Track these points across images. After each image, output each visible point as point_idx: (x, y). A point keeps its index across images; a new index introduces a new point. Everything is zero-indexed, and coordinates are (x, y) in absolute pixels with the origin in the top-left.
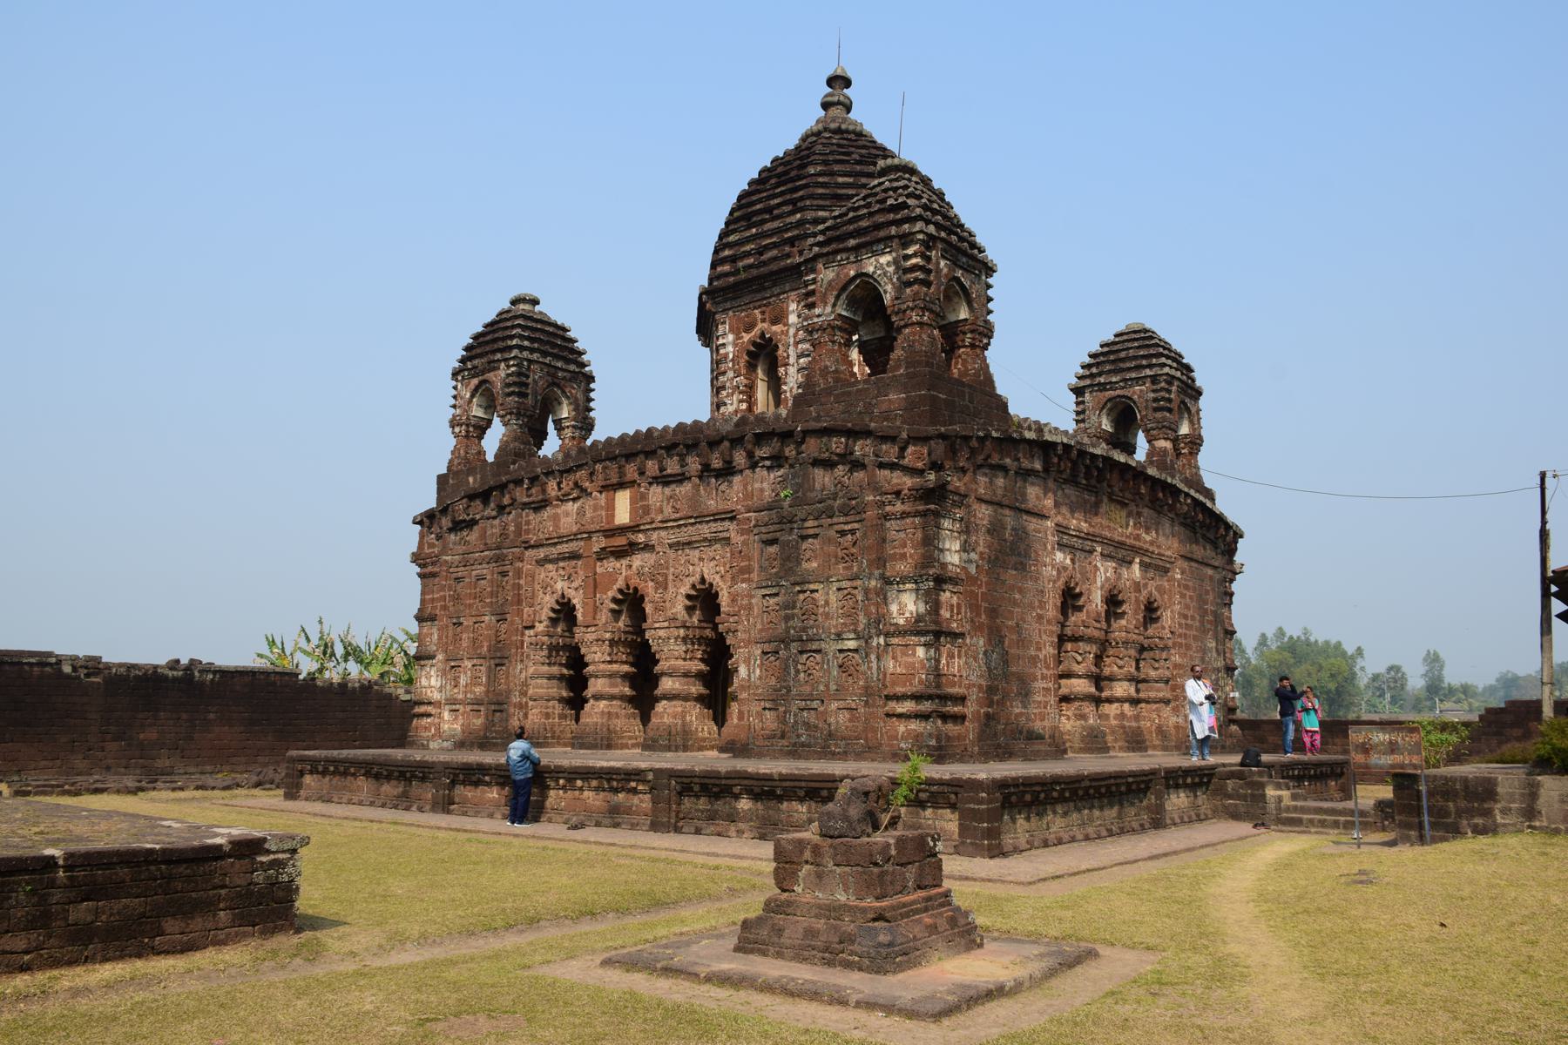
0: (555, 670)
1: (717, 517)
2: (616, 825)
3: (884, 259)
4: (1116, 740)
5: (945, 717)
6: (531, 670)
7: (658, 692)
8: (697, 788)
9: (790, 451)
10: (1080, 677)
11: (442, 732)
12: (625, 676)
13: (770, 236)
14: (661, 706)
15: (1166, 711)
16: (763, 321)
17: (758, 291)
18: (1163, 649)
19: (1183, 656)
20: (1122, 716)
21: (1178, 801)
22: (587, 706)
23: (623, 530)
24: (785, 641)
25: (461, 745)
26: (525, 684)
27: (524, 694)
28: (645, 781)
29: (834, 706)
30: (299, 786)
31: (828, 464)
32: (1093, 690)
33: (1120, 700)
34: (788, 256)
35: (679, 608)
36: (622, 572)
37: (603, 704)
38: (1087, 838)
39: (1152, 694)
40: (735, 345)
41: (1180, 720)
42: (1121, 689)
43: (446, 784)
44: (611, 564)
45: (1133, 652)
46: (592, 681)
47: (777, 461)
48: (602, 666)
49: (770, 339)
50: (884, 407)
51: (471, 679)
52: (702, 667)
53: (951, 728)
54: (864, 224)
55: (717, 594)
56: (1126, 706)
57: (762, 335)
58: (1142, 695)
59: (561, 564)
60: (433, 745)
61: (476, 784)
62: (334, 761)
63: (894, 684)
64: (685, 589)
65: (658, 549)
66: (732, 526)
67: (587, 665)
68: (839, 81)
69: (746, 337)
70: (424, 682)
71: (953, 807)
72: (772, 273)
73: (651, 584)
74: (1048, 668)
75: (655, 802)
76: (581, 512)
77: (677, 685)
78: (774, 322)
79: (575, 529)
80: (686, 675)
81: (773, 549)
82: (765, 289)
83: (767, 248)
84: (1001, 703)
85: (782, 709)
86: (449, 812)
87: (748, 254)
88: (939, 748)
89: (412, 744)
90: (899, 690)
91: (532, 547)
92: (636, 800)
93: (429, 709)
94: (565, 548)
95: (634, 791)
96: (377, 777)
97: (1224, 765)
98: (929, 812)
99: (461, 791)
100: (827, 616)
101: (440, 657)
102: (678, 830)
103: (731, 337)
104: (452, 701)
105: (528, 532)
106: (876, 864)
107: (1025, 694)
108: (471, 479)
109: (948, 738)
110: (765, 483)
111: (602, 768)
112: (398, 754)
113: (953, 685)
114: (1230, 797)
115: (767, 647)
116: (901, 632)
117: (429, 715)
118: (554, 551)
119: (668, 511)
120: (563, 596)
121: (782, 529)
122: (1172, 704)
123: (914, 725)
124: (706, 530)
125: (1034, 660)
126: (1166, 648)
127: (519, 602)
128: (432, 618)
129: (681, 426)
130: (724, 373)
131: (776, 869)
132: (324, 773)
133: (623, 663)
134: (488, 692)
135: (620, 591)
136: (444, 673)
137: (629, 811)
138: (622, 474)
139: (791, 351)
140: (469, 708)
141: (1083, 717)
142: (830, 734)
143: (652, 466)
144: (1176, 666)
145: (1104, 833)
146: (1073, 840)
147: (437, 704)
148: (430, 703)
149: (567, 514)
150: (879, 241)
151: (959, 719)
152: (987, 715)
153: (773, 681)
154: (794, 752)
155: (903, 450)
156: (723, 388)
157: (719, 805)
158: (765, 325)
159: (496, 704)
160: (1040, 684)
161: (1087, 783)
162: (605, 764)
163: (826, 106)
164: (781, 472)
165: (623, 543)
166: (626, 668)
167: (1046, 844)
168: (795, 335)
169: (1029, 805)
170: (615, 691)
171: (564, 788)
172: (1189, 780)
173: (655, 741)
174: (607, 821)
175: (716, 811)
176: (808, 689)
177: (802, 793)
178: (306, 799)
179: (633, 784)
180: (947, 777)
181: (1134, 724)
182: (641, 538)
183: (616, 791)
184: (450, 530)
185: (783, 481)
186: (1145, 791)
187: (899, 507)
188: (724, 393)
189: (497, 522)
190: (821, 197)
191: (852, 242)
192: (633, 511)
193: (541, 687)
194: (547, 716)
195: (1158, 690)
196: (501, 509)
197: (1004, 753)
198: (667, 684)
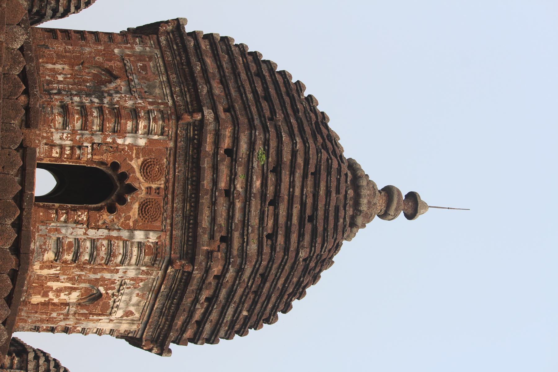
34: (212, 237)
40: (131, 146)
49: (123, 201)
57: (131, 189)
68: (413, 205)
69: (135, 164)
72: (196, 224)
78: (143, 208)
82: (184, 201)
83: (231, 205)
87: (232, 180)
103: (142, 142)
130: (102, 130)
139: (103, 232)
158: (142, 194)
163: (389, 191)
168: (118, 238)
188: (78, 125)
190: (268, 268)
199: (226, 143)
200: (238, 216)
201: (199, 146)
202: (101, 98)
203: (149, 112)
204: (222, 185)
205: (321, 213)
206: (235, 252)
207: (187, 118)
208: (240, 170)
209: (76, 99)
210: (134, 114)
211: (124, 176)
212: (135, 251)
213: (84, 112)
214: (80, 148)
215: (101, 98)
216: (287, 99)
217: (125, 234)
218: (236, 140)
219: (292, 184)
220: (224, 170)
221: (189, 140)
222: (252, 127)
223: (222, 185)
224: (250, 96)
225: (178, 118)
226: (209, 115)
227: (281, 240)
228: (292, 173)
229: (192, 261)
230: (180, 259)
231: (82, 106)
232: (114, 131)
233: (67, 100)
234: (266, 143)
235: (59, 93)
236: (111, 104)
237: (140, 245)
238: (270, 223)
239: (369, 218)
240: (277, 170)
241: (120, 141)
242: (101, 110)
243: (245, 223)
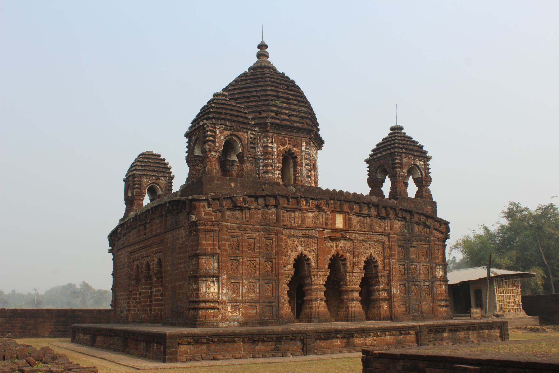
1: (381, 234)
3: (422, 163)
8: (434, 331)
9: (408, 217)
13: (293, 111)
16: (289, 144)
17: (290, 131)
23: (340, 230)
24: (408, 281)
29: (424, 303)
31: (418, 224)
35: (362, 265)
36: (333, 248)
40: (277, 149)
44: (329, 244)
47: (404, 218)
49: (293, 153)
50: (427, 210)
51: (247, 290)
54: (410, 147)
55: (376, 262)
57: (290, 150)
59: (303, 239)
60: (221, 324)
64: (364, 259)
65: (355, 241)
66: (386, 238)
68: (262, 46)
69: (282, 148)
73: (348, 254)
76: (316, 218)
79: (312, 225)
81: (400, 249)
82: (293, 132)
83: (293, 115)
85: (407, 304)
89: (202, 325)
90: (440, 298)
91: (288, 228)
92: (408, 338)
94: (307, 233)
95: (409, 334)
96: (254, 341)
98: (493, 331)
100: (420, 274)
103: (275, 145)
105: (283, 221)
108: (233, 185)
110: (398, 224)
115: (402, 283)
116: (440, 281)
118: (301, 233)
119: (358, 226)
120: (302, 254)
121: (406, 244)
123: (445, 309)
124: (375, 238)
127: (281, 254)
128: (212, 255)
129: (355, 194)
130: (272, 159)
134: (260, 298)
135: (333, 255)
137: (405, 342)
138: (341, 208)
140: (247, 305)
142: (424, 313)
143: (356, 208)
147: (223, 302)
149: (309, 218)
150: (422, 157)
153: (402, 295)
154: (414, 319)
155: (440, 225)
156: (272, 166)
158: (290, 146)
164: (402, 223)
165: (337, 235)
175: (437, 338)
176: (415, 297)
177: (465, 329)
182: (347, 235)
184: (228, 209)
185: (404, 227)
187: (437, 242)
188: (271, 168)
189: (260, 211)
191: (415, 154)
192: (344, 224)
196: (266, 206)
199: (274, 114)
200: (295, 113)
201: (278, 125)
202: (259, 159)
203: (264, 142)
204: (287, 118)
205: (287, 83)
206: (306, 115)
207: (268, 128)
208: (284, 111)
209: (261, 168)
210: (265, 147)
211: (286, 152)
212: (307, 150)
213: (266, 165)
214: (278, 167)
215: (259, 159)
216: (244, 90)
217: (303, 153)
218: (273, 111)
219: (282, 92)
220: (283, 116)
221: (275, 128)
222: (268, 105)
223: (287, 118)
224: (254, 104)
225: (268, 131)
226: (269, 120)
227: (299, 99)
228: (278, 92)
229: (312, 131)
230: (310, 135)
231: (263, 166)
232: (272, 155)
233: (261, 171)
234: (272, 100)
235: (258, 175)
236: (262, 155)
237: (306, 149)
238: (295, 102)
239: (269, 62)
240: (278, 97)
241: (276, 153)
242: (264, 159)
243: (297, 111)
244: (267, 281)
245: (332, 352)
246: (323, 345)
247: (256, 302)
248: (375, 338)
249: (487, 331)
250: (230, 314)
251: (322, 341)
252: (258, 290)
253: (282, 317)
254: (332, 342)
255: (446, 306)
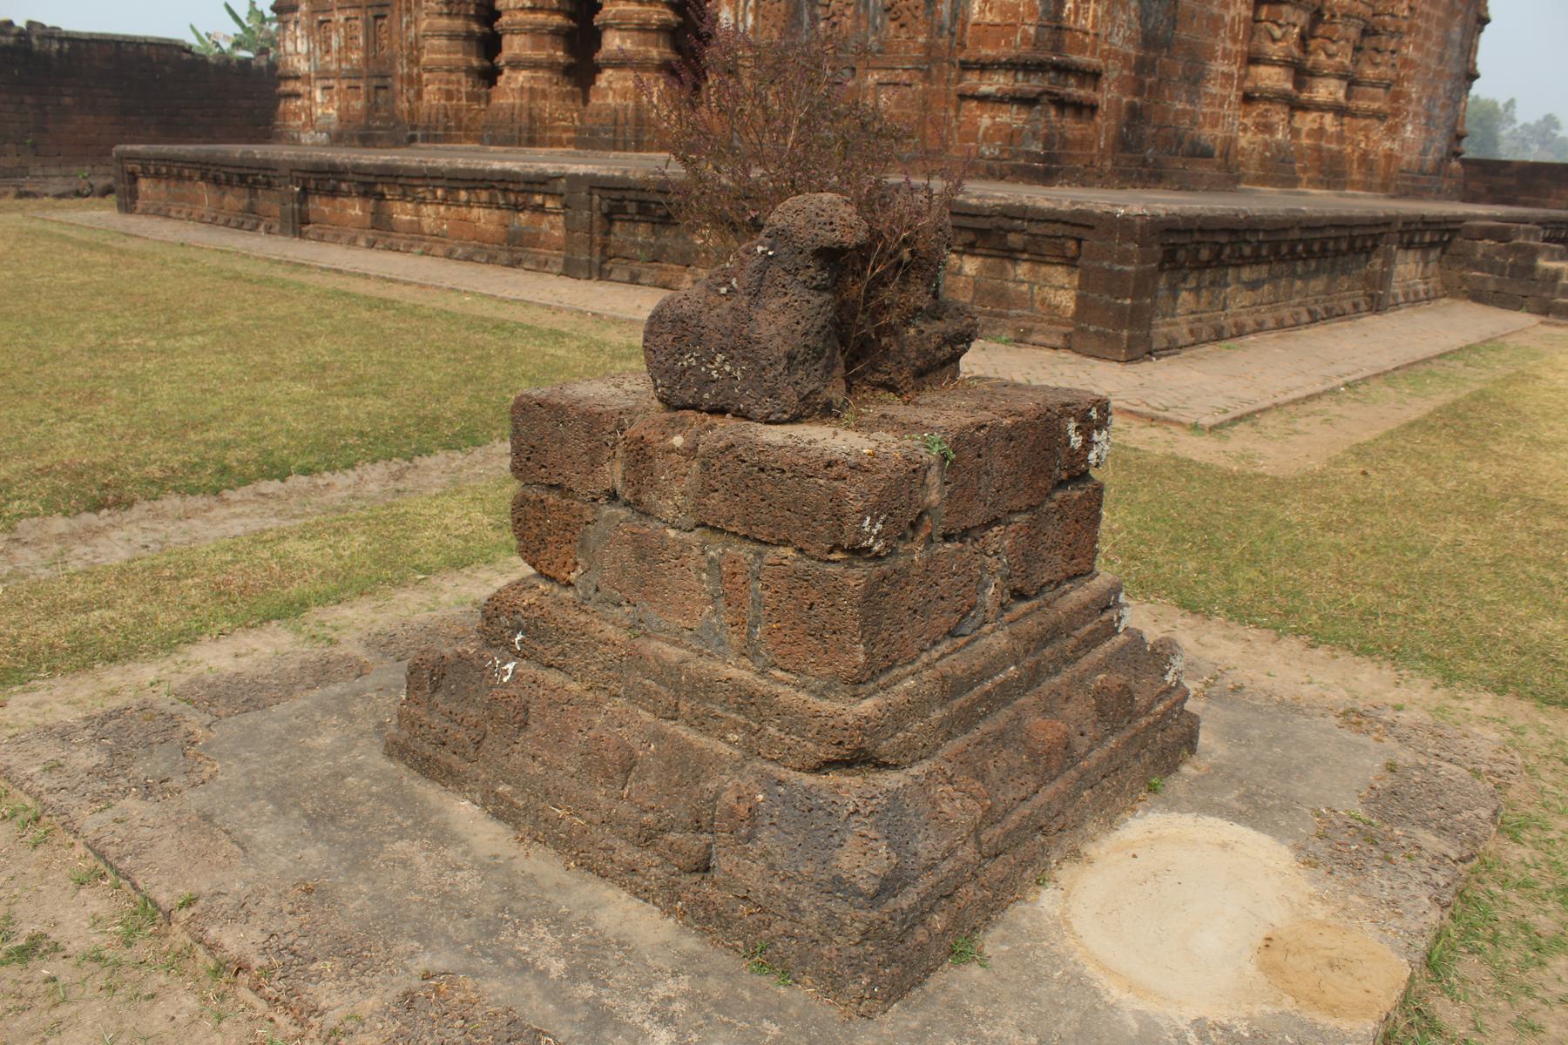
0: (459, 24)
2: (514, 263)
4: (1304, 170)
5: (1062, 104)
6: (424, 25)
7: (599, 57)
8: (632, 208)
10: (1272, 63)
11: (317, 114)
12: (556, 32)
14: (602, 80)
15: (1378, 130)
18: (1392, 35)
19: (1418, 48)
20: (1320, 132)
21: (1407, 269)
22: (501, 80)
25: (337, 139)
26: (416, 47)
27: (414, 61)
28: (553, 195)
29: (873, 78)
30: (133, 195)
32: (1289, 86)
33: (1321, 108)
37: (522, 77)
38: (1280, 325)
39: (1363, 104)
41: (1396, 146)
42: (1326, 90)
43: (300, 197)
45: (1353, 33)
46: (506, 40)
48: (520, 16)
52: (669, 15)
53: (1071, 126)
56: (1329, 119)
58: (1353, 104)
60: (306, 138)
61: (334, 193)
62: (164, 159)
63: (979, 41)
67: (498, 15)
70: (290, 47)
71: (1071, 263)
74: (1234, 40)
75: (569, 229)
77: (628, 45)
80: (643, 28)
84: (1155, 90)
86: (301, 235)
88: (1048, 158)
90: (987, 52)
93: (299, 87)
95: (540, 209)
96: (216, 181)
97: (1476, 217)
98: (1022, 270)
99: (319, 206)
101: (304, 7)
102: (603, 275)
104: (324, 74)
106: (857, 552)
107: (1195, 79)
109: (1065, 143)
111: (493, 172)
112: (258, 151)
113: (1082, 49)
114: (1477, 267)
117: (298, 96)
122: (1390, 121)
123: (1010, 117)
125: (1215, 23)
126: (1397, 33)
131: (520, 503)
132: (157, 175)
133: (553, 11)
134: (366, 59)
136: (310, 33)
141: (1267, 128)
144: (1407, 63)
145: (1305, 318)
146: (1260, 328)
147: (306, 79)
148: (297, 78)
151: (1086, 109)
152: (1134, 113)
157: (668, 237)
159: (377, 77)
160: (1219, 66)
161: (1295, 234)
162: (497, 166)
166: (558, 20)
167: (1219, 336)
169: (1202, 267)
170: (542, 55)
171: (444, 201)
172: (1427, 238)
173: (593, 132)
174: (504, 256)
175: (663, 248)
178: (145, 213)
179: (538, 199)
180: (1065, 206)
181: (1334, 146)
183: (517, 208)
186: (1368, 252)
193: (437, 51)
194: (449, 95)
195: (1373, 99)
197: (1153, 176)
198: (613, 42)
244: (377, 11)
245: (336, 239)
246: (327, 210)
247: (355, 75)
248: (442, 209)
249: (971, 266)
250: (320, 111)
251: (324, 199)
252: (361, 40)
253: (398, 123)
254: (344, 208)
255: (1025, 101)
